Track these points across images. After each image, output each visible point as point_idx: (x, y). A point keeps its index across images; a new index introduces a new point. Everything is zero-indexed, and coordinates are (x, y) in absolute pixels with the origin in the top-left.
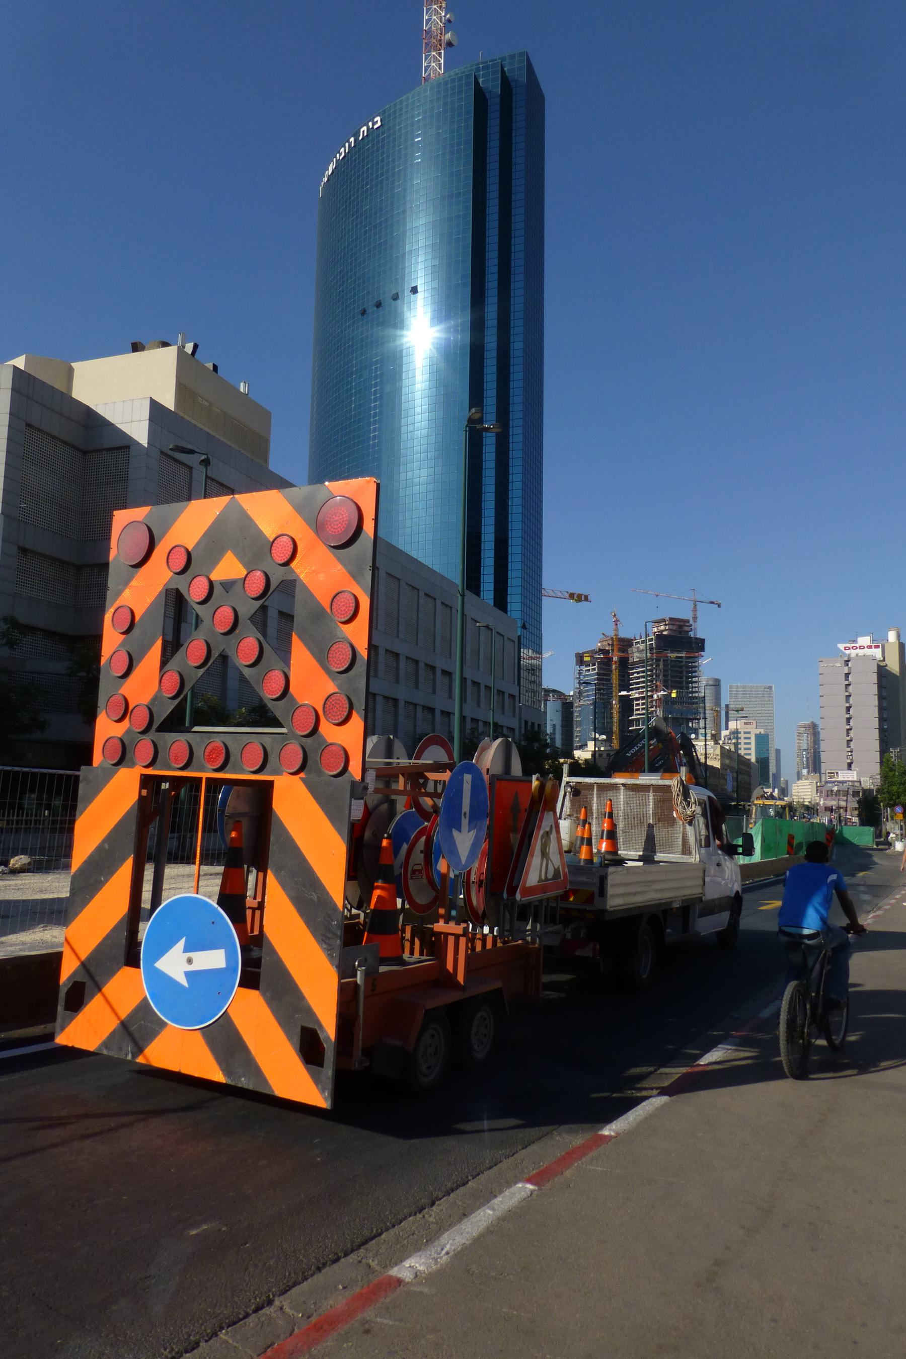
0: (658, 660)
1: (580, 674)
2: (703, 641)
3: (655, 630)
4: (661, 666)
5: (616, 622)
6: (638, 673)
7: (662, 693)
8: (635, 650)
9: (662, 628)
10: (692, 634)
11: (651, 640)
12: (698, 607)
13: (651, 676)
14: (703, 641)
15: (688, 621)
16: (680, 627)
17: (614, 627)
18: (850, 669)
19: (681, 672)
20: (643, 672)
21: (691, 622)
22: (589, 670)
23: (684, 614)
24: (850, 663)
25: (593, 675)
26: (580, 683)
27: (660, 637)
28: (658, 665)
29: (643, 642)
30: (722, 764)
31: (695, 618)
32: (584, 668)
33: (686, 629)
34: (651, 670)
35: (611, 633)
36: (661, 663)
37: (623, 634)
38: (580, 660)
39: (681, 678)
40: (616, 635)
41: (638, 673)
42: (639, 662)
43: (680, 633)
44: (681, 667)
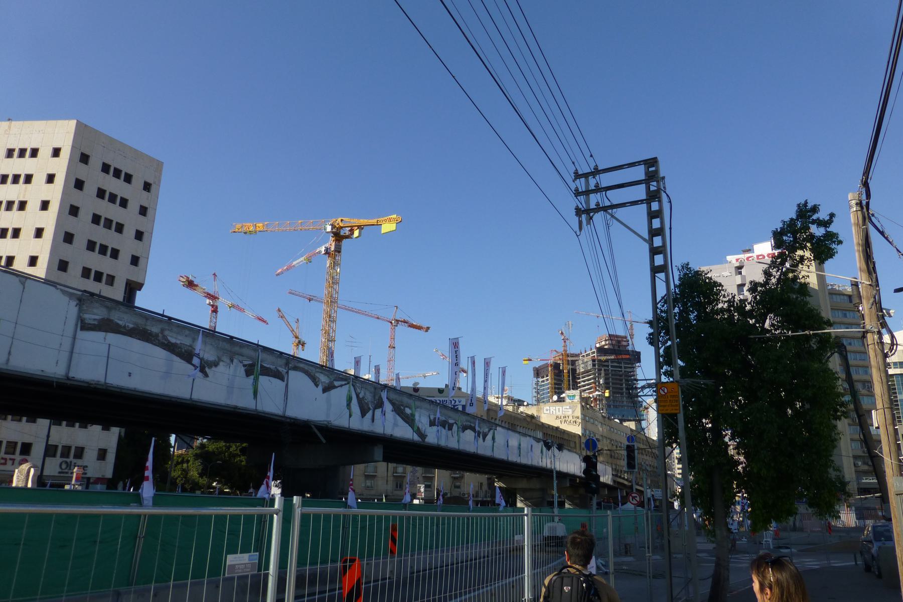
0: (600, 370)
1: (537, 384)
2: (639, 353)
3: (598, 345)
4: (603, 375)
5: (565, 340)
7: (597, 393)
8: (580, 362)
9: (603, 343)
10: (630, 348)
12: (634, 327)
13: (595, 383)
14: (639, 354)
15: (626, 337)
16: (619, 342)
17: (563, 344)
18: (744, 278)
19: (621, 380)
20: (588, 380)
21: (629, 338)
23: (620, 332)
24: (743, 271)
26: (538, 393)
27: (601, 350)
28: (600, 374)
29: (587, 355)
30: (584, 429)
31: (632, 336)
32: (541, 380)
33: (625, 343)
35: (561, 350)
37: (572, 350)
38: (538, 373)
39: (622, 385)
42: (583, 373)
44: (621, 376)
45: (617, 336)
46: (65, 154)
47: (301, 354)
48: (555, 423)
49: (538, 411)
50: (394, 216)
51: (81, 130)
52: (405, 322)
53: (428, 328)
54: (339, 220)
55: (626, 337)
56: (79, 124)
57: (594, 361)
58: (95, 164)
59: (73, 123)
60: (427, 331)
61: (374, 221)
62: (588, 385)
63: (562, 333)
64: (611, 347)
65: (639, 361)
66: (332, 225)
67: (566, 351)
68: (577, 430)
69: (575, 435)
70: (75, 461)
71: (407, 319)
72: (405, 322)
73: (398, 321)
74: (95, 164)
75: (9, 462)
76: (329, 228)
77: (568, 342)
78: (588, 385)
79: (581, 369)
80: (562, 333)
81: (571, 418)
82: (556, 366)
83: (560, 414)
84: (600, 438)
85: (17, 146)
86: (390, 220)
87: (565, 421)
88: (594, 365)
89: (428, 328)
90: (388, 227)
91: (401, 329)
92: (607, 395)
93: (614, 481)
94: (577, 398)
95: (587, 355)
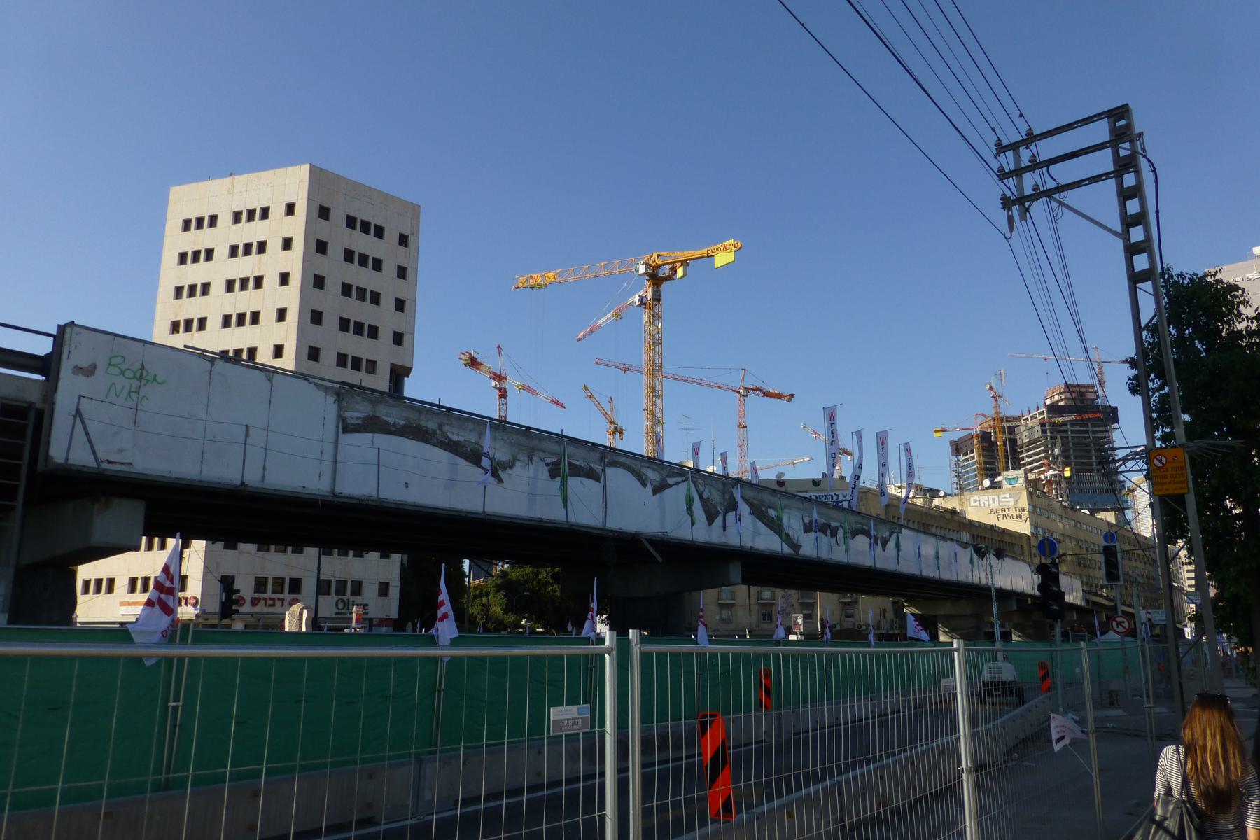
0: (1053, 438)
1: (957, 464)
2: (1115, 410)
3: (1048, 402)
6: (1030, 456)
7: (1051, 472)
8: (1022, 428)
9: (1057, 398)
10: (1099, 402)
11: (1042, 413)
13: (1047, 458)
14: (1115, 410)
15: (1093, 387)
16: (1082, 394)
17: (994, 404)
19: (1090, 451)
21: (1098, 387)
22: (967, 460)
23: (1084, 378)
25: (974, 464)
26: (960, 478)
27: (1053, 409)
29: (1032, 418)
30: (1035, 526)
31: (1102, 384)
32: (962, 458)
34: (1043, 451)
35: (991, 412)
36: (1058, 441)
37: (1009, 411)
38: (958, 448)
39: (1090, 458)
40: (998, 413)
41: (1030, 456)
42: (1028, 444)
43: (1082, 401)
44: (1087, 445)
45: (1078, 386)
46: (301, 210)
47: (620, 445)
48: (990, 520)
49: (962, 503)
50: (731, 242)
51: (317, 176)
52: (758, 390)
53: (792, 396)
54: (655, 255)
55: (1093, 387)
56: (312, 167)
57: (1043, 425)
58: (338, 217)
59: (306, 168)
60: (790, 400)
61: (703, 252)
62: (1037, 461)
63: (991, 388)
64: (1070, 403)
65: (1117, 421)
66: (646, 264)
67: (998, 413)
68: (1024, 528)
69: (1021, 536)
70: (352, 598)
71: (760, 385)
72: (758, 390)
73: (747, 389)
74: (338, 217)
75: (278, 603)
76: (642, 269)
77: (1000, 401)
78: (1037, 461)
79: (1024, 438)
80: (991, 388)
81: (1013, 511)
82: (985, 437)
83: (995, 506)
84: (1061, 539)
85: (244, 207)
86: (725, 248)
87: (1005, 516)
88: (1044, 432)
89: (792, 396)
90: (723, 258)
91: (754, 398)
92: (1067, 474)
93: (1087, 601)
94: (1021, 482)
95: (1032, 418)
